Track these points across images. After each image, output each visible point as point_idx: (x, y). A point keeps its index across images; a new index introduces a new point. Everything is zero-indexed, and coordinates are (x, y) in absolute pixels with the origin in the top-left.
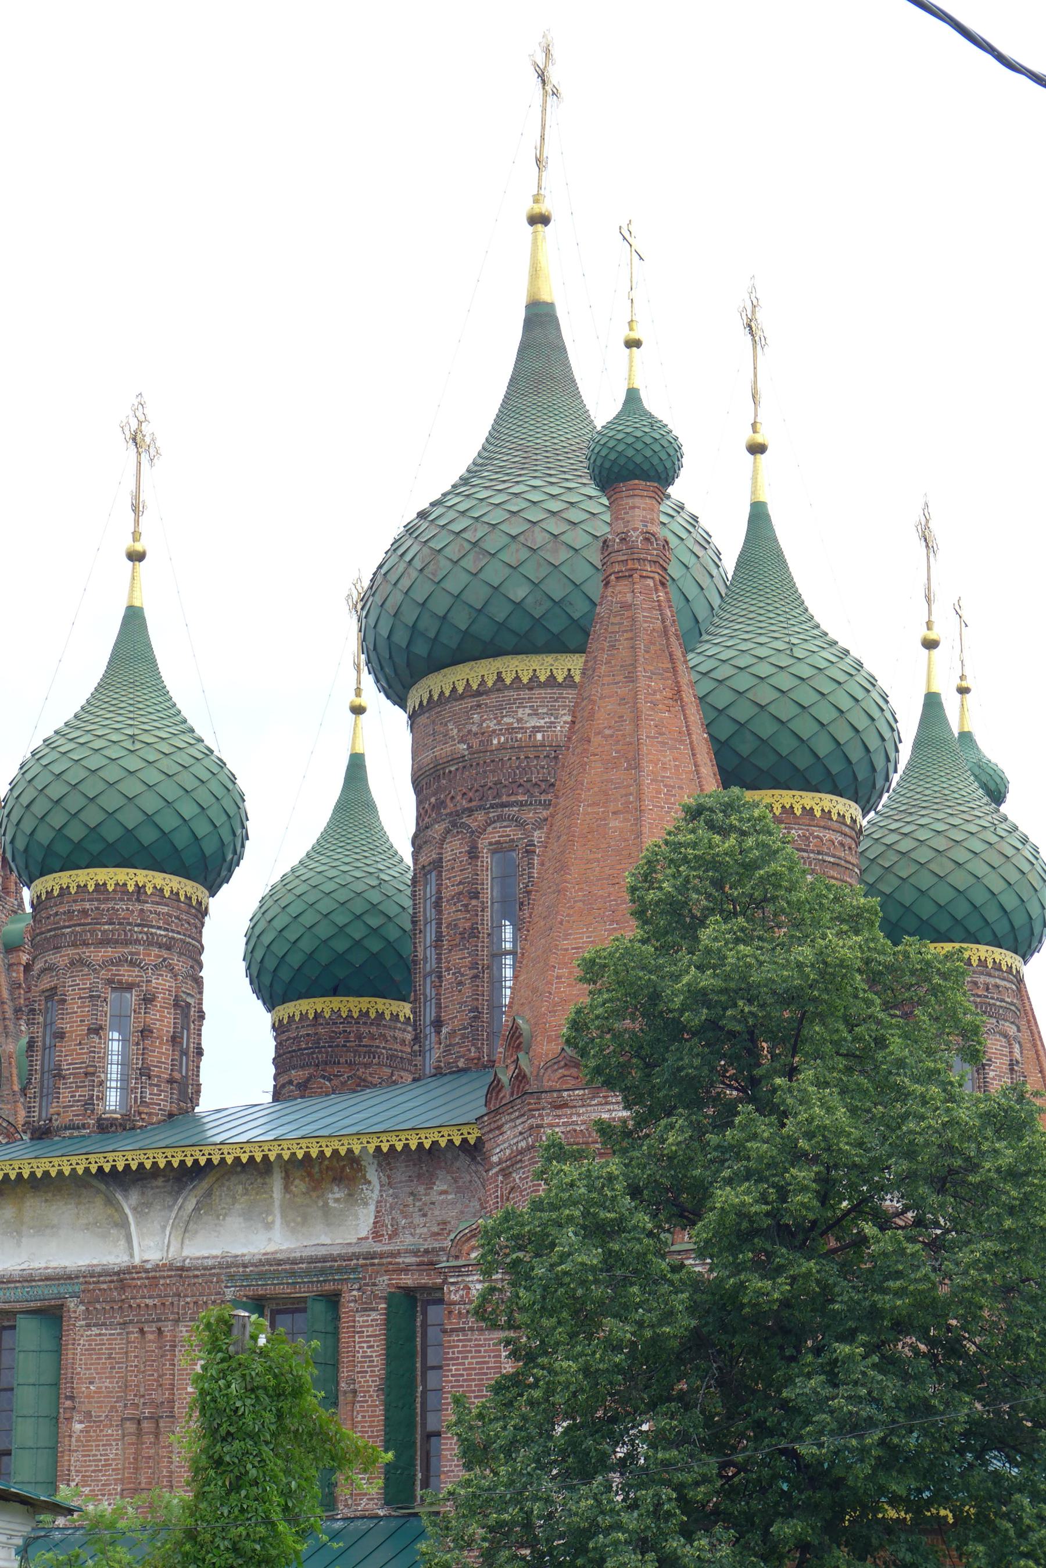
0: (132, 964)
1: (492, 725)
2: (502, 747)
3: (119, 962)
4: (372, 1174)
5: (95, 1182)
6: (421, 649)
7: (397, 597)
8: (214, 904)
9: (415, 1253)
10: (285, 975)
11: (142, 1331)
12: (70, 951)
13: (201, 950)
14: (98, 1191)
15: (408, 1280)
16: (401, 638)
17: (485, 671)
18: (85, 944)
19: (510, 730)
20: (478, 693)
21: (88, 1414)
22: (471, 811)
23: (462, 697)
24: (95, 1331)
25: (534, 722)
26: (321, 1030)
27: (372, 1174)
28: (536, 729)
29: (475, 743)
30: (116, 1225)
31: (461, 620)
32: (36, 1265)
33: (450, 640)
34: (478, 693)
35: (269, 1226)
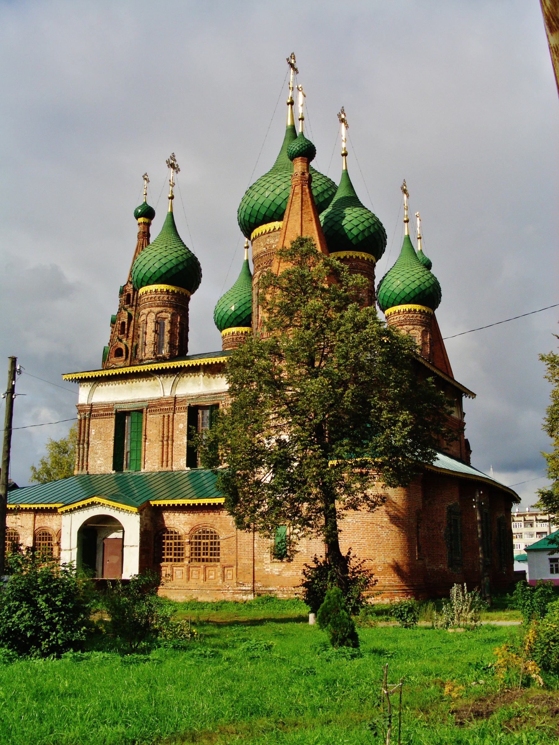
0: (166, 312)
1: (272, 242)
3: (162, 312)
6: (253, 220)
7: (245, 206)
8: (192, 297)
10: (224, 322)
11: (164, 416)
12: (148, 309)
13: (188, 310)
16: (247, 218)
18: (152, 307)
20: (269, 233)
23: (264, 234)
24: (152, 416)
26: (234, 337)
29: (268, 247)
30: (157, 386)
31: (263, 211)
32: (136, 398)
33: (260, 218)
34: (269, 233)
35: (199, 385)
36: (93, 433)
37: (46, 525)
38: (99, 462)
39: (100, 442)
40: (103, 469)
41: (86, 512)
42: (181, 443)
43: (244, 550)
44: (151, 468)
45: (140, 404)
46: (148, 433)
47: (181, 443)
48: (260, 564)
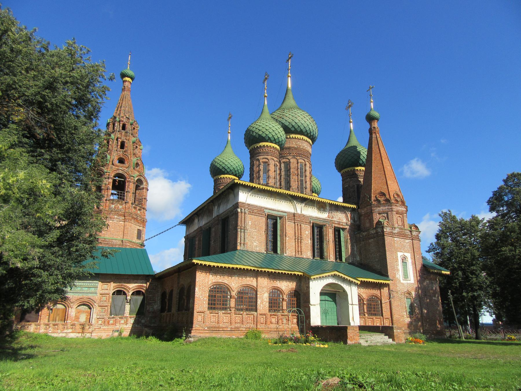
2: (302, 148)
4: (328, 208)
5: (289, 197)
9: (337, 222)
12: (270, 157)
14: (289, 199)
15: (336, 225)
17: (302, 137)
19: (303, 146)
20: (299, 139)
21: (289, 237)
22: (297, 156)
24: (289, 222)
25: (306, 146)
27: (328, 208)
28: (306, 148)
36: (250, 224)
37: (277, 286)
38: (255, 244)
39: (255, 230)
40: (258, 249)
41: (325, 280)
42: (308, 242)
43: (396, 310)
44: (290, 254)
45: (282, 214)
46: (287, 232)
47: (308, 242)
48: (403, 317)
